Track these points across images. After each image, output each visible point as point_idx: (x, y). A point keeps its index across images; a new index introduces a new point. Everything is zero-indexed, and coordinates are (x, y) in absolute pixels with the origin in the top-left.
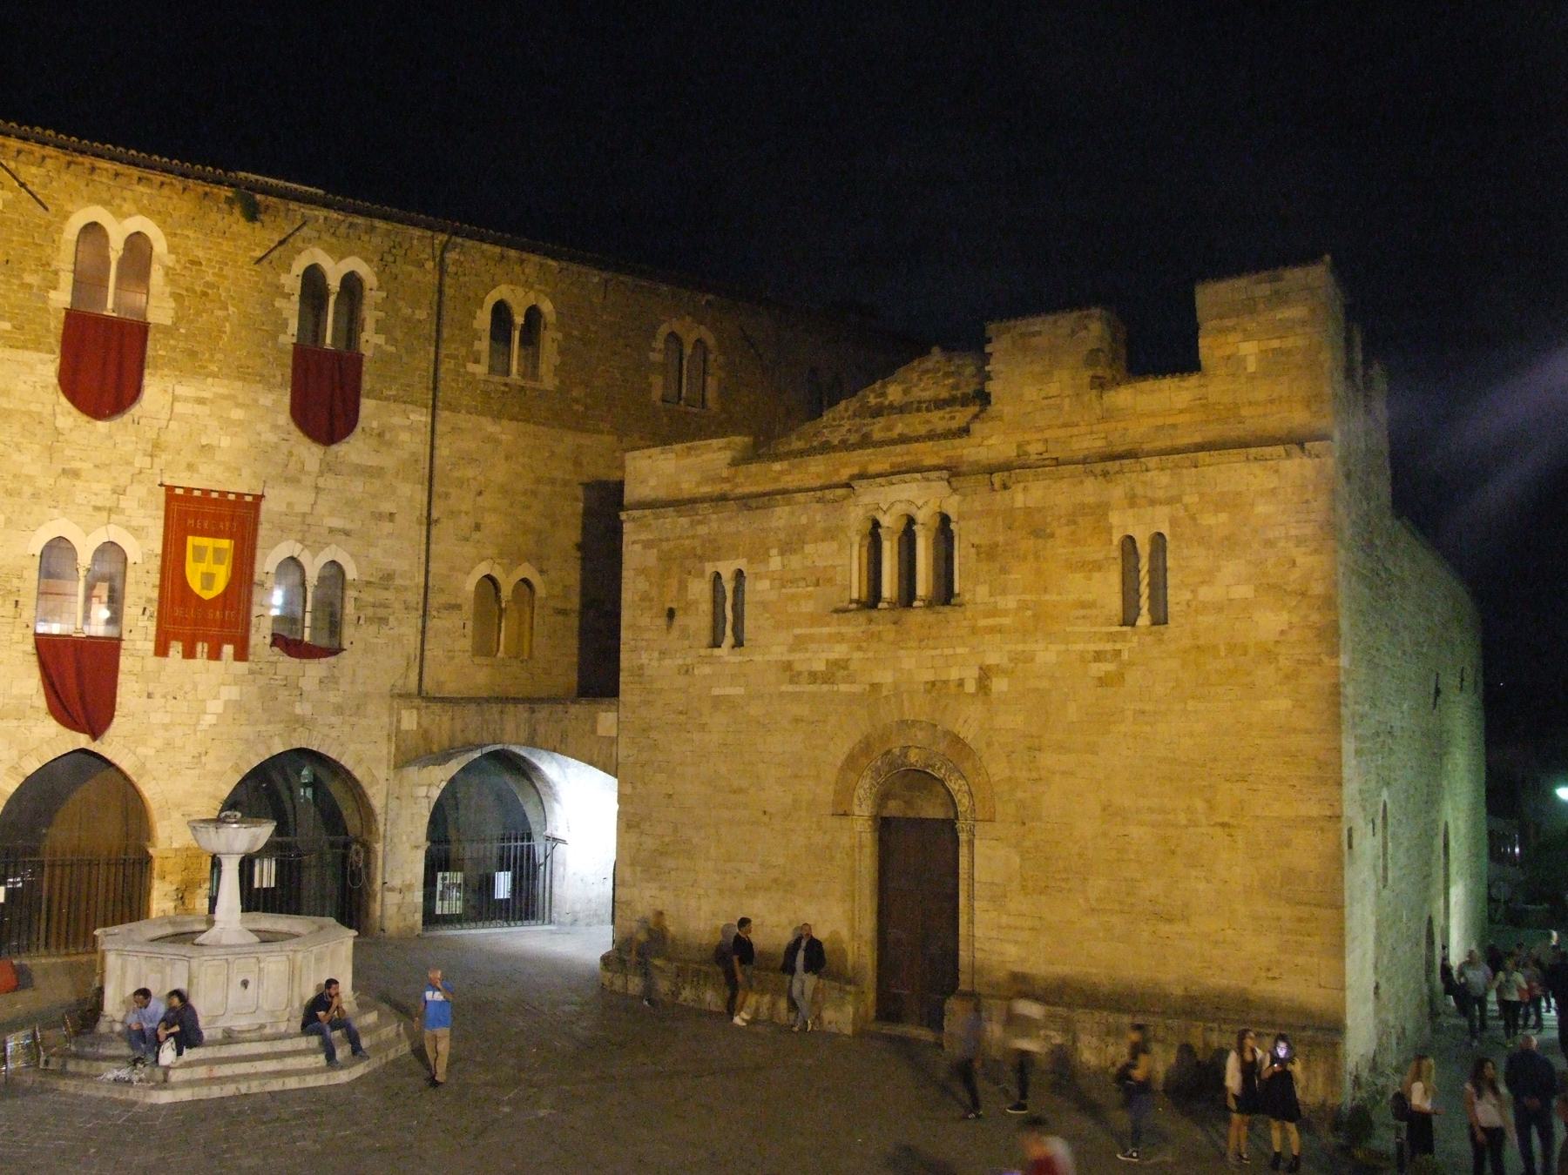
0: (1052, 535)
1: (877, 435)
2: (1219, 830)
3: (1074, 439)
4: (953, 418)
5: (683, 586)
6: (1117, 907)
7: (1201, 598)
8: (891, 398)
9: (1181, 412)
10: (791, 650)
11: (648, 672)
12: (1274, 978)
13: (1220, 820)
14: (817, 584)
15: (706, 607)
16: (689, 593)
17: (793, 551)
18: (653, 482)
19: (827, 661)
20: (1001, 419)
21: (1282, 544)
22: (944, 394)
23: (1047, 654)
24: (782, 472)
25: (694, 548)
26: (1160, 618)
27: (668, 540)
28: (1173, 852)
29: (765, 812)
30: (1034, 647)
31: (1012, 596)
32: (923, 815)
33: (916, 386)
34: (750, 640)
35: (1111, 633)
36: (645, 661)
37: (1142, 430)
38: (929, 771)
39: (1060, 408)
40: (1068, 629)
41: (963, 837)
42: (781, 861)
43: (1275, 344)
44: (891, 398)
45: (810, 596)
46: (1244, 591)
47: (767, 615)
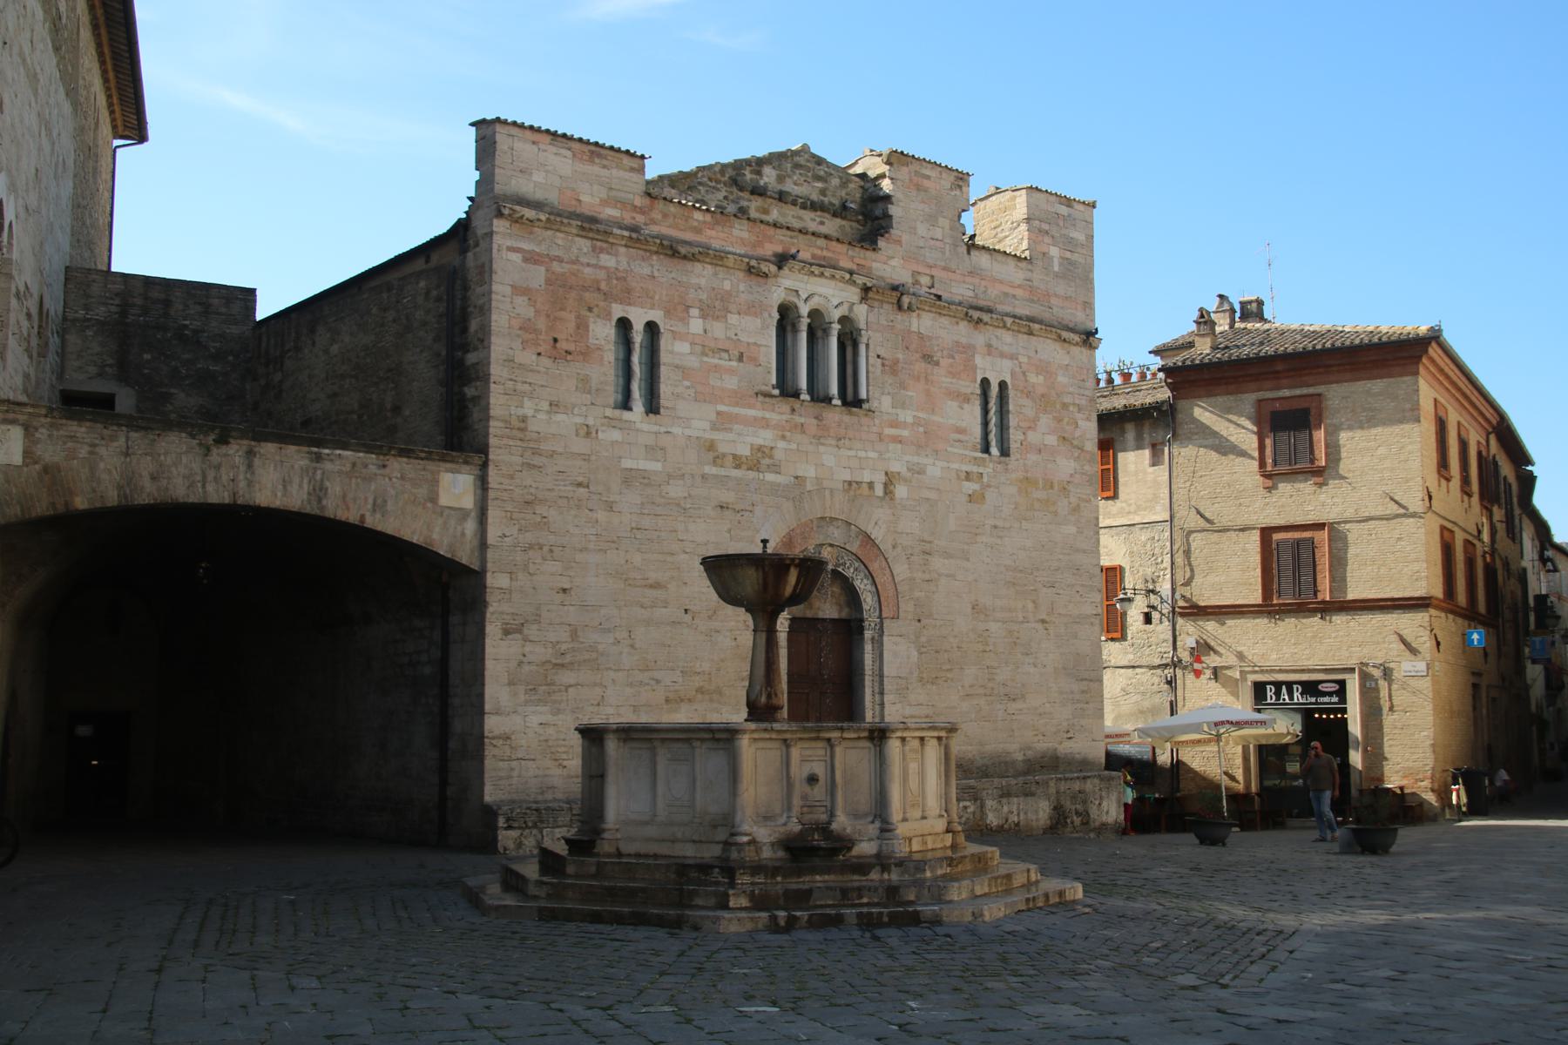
0: (937, 364)
1: (753, 214)
2: (1040, 626)
3: (953, 284)
4: (822, 223)
5: (582, 326)
6: (981, 691)
7: (1029, 439)
8: (766, 179)
9: (1019, 286)
10: (714, 428)
11: (533, 426)
12: (1070, 738)
13: (1041, 617)
14: (740, 358)
15: (610, 354)
16: (591, 333)
17: (717, 318)
18: (538, 177)
19: (752, 445)
20: (899, 242)
21: (1071, 408)
22: (815, 197)
23: (935, 470)
24: (705, 222)
25: (598, 282)
26: (1005, 452)
27: (560, 260)
28: (1015, 643)
29: (686, 611)
30: (925, 461)
31: (909, 412)
32: (821, 615)
33: (789, 177)
34: (667, 408)
35: (975, 458)
36: (530, 413)
37: (995, 292)
38: (840, 569)
39: (944, 253)
40: (949, 449)
41: (868, 634)
42: (706, 666)
43: (1068, 255)
44: (766, 179)
45: (731, 371)
46: (1051, 440)
47: (687, 383)
